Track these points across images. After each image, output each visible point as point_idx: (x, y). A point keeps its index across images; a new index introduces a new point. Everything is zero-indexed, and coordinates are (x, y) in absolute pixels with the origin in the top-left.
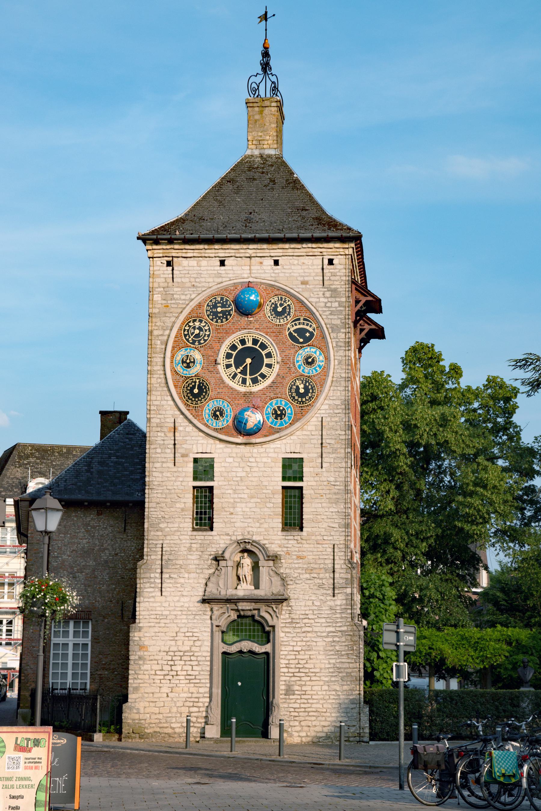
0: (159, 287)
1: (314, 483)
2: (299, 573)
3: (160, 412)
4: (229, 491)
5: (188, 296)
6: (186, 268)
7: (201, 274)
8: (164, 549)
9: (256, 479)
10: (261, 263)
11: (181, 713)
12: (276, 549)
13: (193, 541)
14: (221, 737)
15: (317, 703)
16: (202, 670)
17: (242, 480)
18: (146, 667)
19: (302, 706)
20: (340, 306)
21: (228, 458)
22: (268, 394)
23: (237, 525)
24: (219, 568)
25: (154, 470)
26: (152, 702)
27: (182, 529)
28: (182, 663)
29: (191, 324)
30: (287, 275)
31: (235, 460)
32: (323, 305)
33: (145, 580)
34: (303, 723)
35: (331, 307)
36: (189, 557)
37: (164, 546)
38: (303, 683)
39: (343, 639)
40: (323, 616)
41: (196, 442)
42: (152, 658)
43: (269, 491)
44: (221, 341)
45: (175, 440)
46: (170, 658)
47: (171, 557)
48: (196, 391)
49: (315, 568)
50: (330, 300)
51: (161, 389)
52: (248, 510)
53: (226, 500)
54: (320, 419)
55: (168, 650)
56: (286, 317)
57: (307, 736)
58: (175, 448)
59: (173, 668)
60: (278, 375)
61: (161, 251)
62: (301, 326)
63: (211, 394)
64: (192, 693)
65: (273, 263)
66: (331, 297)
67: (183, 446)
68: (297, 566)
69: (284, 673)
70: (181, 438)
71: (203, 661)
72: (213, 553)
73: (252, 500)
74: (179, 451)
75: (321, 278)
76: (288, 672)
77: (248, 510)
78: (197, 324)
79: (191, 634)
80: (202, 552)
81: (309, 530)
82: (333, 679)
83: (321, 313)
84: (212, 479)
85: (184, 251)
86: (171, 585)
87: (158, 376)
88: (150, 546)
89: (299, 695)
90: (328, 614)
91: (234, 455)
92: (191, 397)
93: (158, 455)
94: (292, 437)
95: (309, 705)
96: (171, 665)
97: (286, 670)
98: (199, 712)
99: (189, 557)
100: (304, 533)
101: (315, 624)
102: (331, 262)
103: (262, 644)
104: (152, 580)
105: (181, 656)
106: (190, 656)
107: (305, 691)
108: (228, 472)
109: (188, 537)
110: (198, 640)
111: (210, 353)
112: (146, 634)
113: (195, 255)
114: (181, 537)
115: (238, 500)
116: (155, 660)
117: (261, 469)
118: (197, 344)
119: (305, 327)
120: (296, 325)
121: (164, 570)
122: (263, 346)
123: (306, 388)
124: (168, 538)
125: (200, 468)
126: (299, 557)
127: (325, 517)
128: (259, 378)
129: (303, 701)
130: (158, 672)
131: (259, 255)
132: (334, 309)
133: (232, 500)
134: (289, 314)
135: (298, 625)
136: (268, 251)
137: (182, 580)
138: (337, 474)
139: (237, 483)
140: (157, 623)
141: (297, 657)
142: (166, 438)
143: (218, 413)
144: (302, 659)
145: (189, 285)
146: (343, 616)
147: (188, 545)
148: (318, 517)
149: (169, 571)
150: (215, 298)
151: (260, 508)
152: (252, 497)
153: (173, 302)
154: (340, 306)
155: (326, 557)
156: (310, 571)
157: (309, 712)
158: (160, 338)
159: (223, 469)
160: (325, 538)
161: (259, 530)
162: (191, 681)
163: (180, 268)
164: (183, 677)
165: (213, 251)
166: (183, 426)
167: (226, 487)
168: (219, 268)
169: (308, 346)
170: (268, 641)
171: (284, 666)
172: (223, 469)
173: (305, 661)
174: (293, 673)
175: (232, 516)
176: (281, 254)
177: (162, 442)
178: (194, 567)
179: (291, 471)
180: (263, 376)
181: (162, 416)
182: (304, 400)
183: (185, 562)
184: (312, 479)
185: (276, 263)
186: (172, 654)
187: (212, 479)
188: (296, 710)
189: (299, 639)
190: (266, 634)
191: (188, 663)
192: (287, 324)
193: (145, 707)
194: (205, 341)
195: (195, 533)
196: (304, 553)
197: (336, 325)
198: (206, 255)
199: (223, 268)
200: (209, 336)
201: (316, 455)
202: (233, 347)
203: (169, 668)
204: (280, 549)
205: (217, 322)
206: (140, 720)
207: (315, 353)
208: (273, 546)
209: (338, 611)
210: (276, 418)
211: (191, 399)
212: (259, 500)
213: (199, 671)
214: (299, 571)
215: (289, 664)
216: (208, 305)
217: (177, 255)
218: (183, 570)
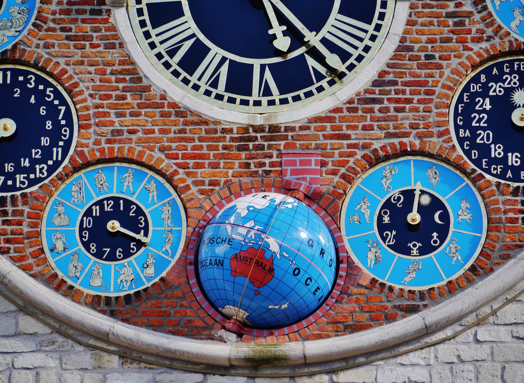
22: (356, 136)
60: (403, 48)
63: (83, 140)
143: (114, 226)
210: (401, 247)
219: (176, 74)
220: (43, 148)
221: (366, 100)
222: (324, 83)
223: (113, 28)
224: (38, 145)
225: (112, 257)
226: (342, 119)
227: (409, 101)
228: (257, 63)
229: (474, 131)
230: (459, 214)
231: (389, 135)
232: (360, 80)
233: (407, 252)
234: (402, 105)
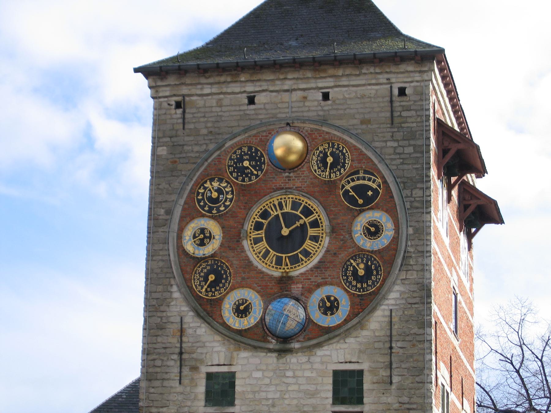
5: (204, 147)
6: (201, 110)
7: (221, 116)
10: (305, 98)
20: (415, 152)
29: (208, 185)
31: (266, 374)
32: (391, 151)
35: (403, 153)
48: (212, 278)
50: (401, 143)
51: (163, 276)
54: (388, 313)
56: (339, 170)
60: (327, 251)
61: (168, 89)
62: (361, 182)
65: (321, 98)
75: (388, 114)
78: (216, 184)
83: (388, 162)
85: (199, 87)
87: (160, 258)
91: (264, 367)
93: (158, 370)
94: (347, 341)
102: (402, 92)
111: (232, 222)
113: (214, 90)
117: (302, 387)
118: (214, 212)
119: (366, 182)
120: (353, 180)
122: (307, 212)
123: (368, 270)
125: (216, 387)
128: (300, 256)
132: (408, 156)
134: (344, 166)
136: (313, 81)
138: (412, 392)
145: (204, 131)
150: (241, 149)
154: (415, 152)
158: (164, 205)
165: (238, 84)
168: (245, 107)
169: (371, 209)
176: (332, 84)
179: (346, 389)
180: (307, 254)
182: (365, 285)
185: (326, 96)
192: (340, 180)
197: (411, 179)
198: (229, 90)
199: (252, 107)
200: (231, 200)
202: (265, 215)
205: (243, 180)
207: (380, 218)
216: (231, 159)
217: (189, 93)
219: (260, 259)
220: (223, 283)
221: (316, 267)
222: (303, 262)
223: (243, 246)
224: (221, 282)
225: (242, 317)
226: (309, 274)
227: (328, 268)
228: (284, 256)
229: (347, 277)
231: (322, 279)
232: (315, 260)
233: (327, 315)
234: (326, 268)
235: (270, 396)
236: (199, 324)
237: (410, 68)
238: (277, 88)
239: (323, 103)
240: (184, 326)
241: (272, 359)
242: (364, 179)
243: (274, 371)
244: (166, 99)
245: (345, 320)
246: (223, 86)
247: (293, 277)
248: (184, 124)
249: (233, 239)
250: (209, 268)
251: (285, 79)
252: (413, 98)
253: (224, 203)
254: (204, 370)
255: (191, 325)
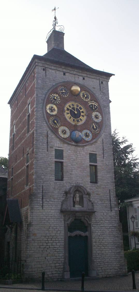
0: (40, 78)
1: (101, 164)
2: (98, 201)
3: (41, 128)
4: (70, 165)
5: (52, 84)
8: (44, 188)
9: (80, 160)
11: (51, 267)
12: (89, 190)
13: (56, 185)
14: (71, 277)
15: (107, 259)
16: (61, 245)
17: (74, 160)
18: (36, 244)
19: (102, 260)
21: (69, 151)
23: (73, 179)
24: (67, 197)
25: (39, 152)
26: (38, 262)
27: (51, 179)
28: (52, 242)
30: (88, 84)
33: (35, 202)
34: (103, 268)
36: (54, 192)
37: (44, 186)
38: (102, 250)
39: (115, 230)
40: (108, 220)
41: (56, 142)
42: (38, 239)
43: (85, 166)
44: (65, 104)
45: (47, 140)
46: (46, 239)
47: (46, 192)
49: (104, 199)
52: (77, 173)
53: (69, 168)
54: (102, 139)
55: (45, 235)
57: (105, 274)
58: (48, 144)
59: (48, 244)
60: (86, 120)
64: (56, 256)
65: (82, 79)
66: (103, 95)
67: (51, 143)
68: (97, 198)
69: (94, 245)
70: (50, 140)
71: (61, 240)
72: (64, 191)
73: (79, 169)
74: (50, 145)
75: (99, 88)
76: (96, 245)
77: (77, 173)
79: (55, 228)
80: (60, 190)
81: (100, 183)
82: (113, 247)
84: (63, 159)
85: (51, 66)
86: (47, 205)
87: (40, 113)
88: (38, 186)
89: (100, 255)
90: (109, 219)
92: (53, 124)
93: (40, 146)
94: (93, 145)
95: (104, 260)
96: (47, 243)
97: (94, 244)
98: (60, 266)
99: (54, 192)
100: (99, 184)
101: (105, 223)
102: (102, 82)
103: (85, 232)
104: (38, 202)
105: (51, 238)
106: (55, 238)
107: (103, 253)
108: (69, 156)
109: (53, 183)
110: (59, 230)
112: (35, 228)
113: (55, 68)
114: (51, 183)
115: (73, 169)
116: (40, 240)
118: (55, 103)
121: (44, 198)
124: (45, 183)
126: (97, 194)
127: (106, 178)
129: (102, 258)
130: (41, 247)
131: (78, 74)
133: (71, 168)
135: (98, 224)
136: (81, 73)
137: (51, 202)
139: (72, 161)
140: (40, 222)
141: (99, 238)
142: (44, 139)
143: (64, 132)
144: (101, 239)
145: (52, 79)
146: (115, 219)
147: (54, 187)
148: (103, 178)
149: (45, 198)
151: (82, 173)
152: (79, 168)
153: (46, 84)
155: (107, 195)
156: (101, 200)
157: (104, 263)
158: (41, 98)
159: (67, 155)
160: (106, 187)
161: (82, 182)
162: (56, 251)
163: (48, 72)
164: (52, 249)
165: (61, 69)
166: (50, 135)
167: (69, 163)
168: (63, 76)
169: (96, 111)
170: (87, 231)
171: (94, 242)
172: (67, 155)
173: (102, 240)
174: (98, 245)
175: (71, 175)
176: (86, 76)
177: (42, 141)
178: (56, 196)
180: (81, 120)
181: (42, 130)
182: (95, 131)
183: (52, 194)
184: (100, 162)
185: (84, 79)
186: (47, 237)
187: (63, 159)
188: (100, 262)
189: (99, 230)
190: (85, 227)
191: (54, 242)
193: (35, 265)
194: (59, 102)
195: (56, 181)
196: (99, 193)
198: (59, 70)
199: (65, 76)
200: (60, 100)
201: (101, 153)
203: (46, 244)
204: (90, 190)
206: (32, 271)
208: (88, 189)
209: (113, 218)
211: (53, 125)
212: (81, 169)
213: (59, 245)
214: (98, 200)
215: (96, 241)
217: (48, 67)
218: (51, 198)
228: (75, 119)
230: (91, 135)
232: (83, 122)
235: (73, 158)
236: (52, 134)
237: (105, 77)
238: (72, 73)
239: (83, 80)
240: (48, 134)
241: (73, 148)
242: (94, 103)
243: (74, 151)
244: (40, 67)
245: (91, 140)
246: (57, 68)
247: (78, 125)
248: (46, 75)
249: (61, 111)
250: (54, 118)
251: (74, 71)
252: (105, 85)
253: (58, 101)
254: (55, 148)
255: (50, 134)
